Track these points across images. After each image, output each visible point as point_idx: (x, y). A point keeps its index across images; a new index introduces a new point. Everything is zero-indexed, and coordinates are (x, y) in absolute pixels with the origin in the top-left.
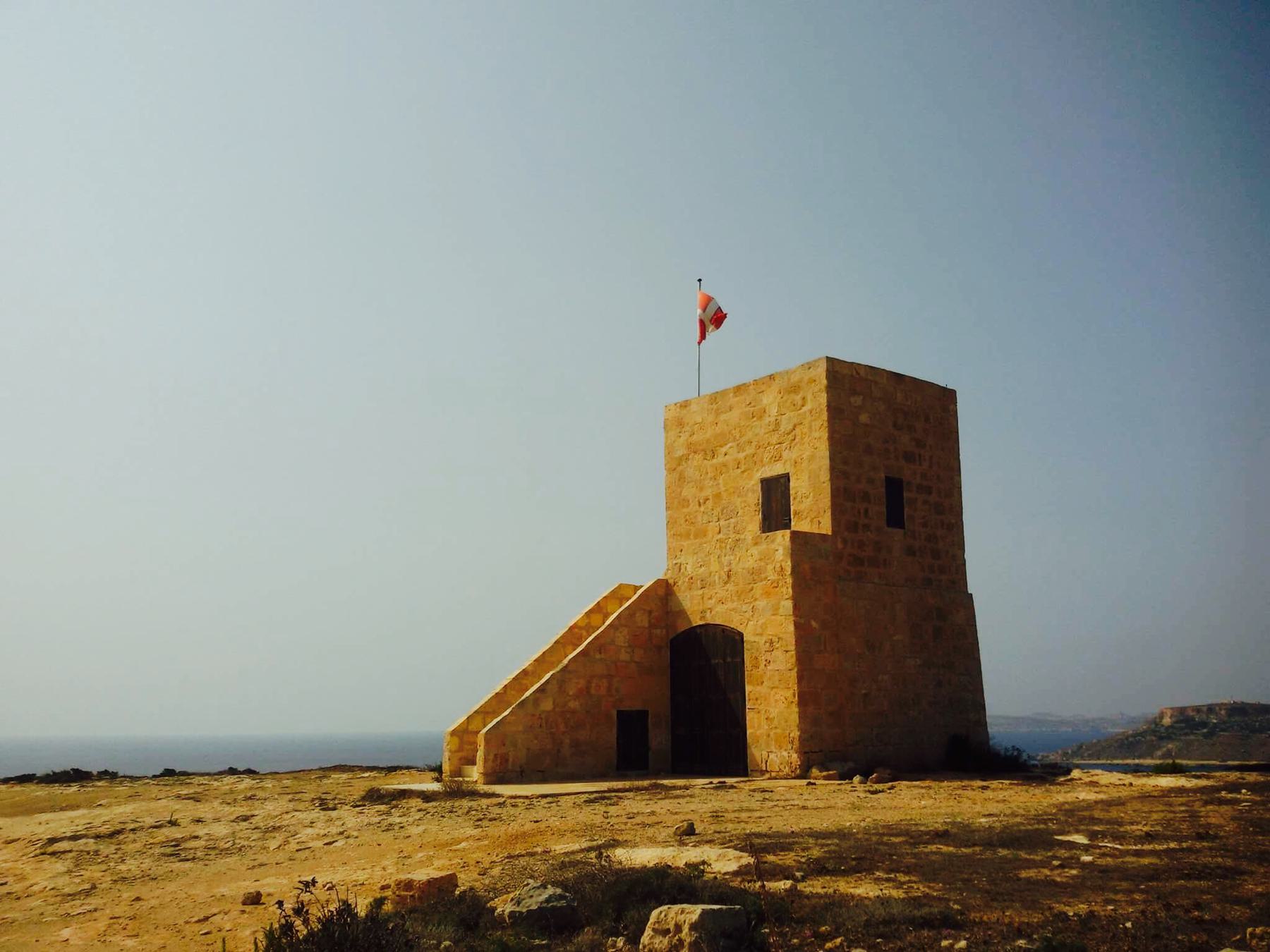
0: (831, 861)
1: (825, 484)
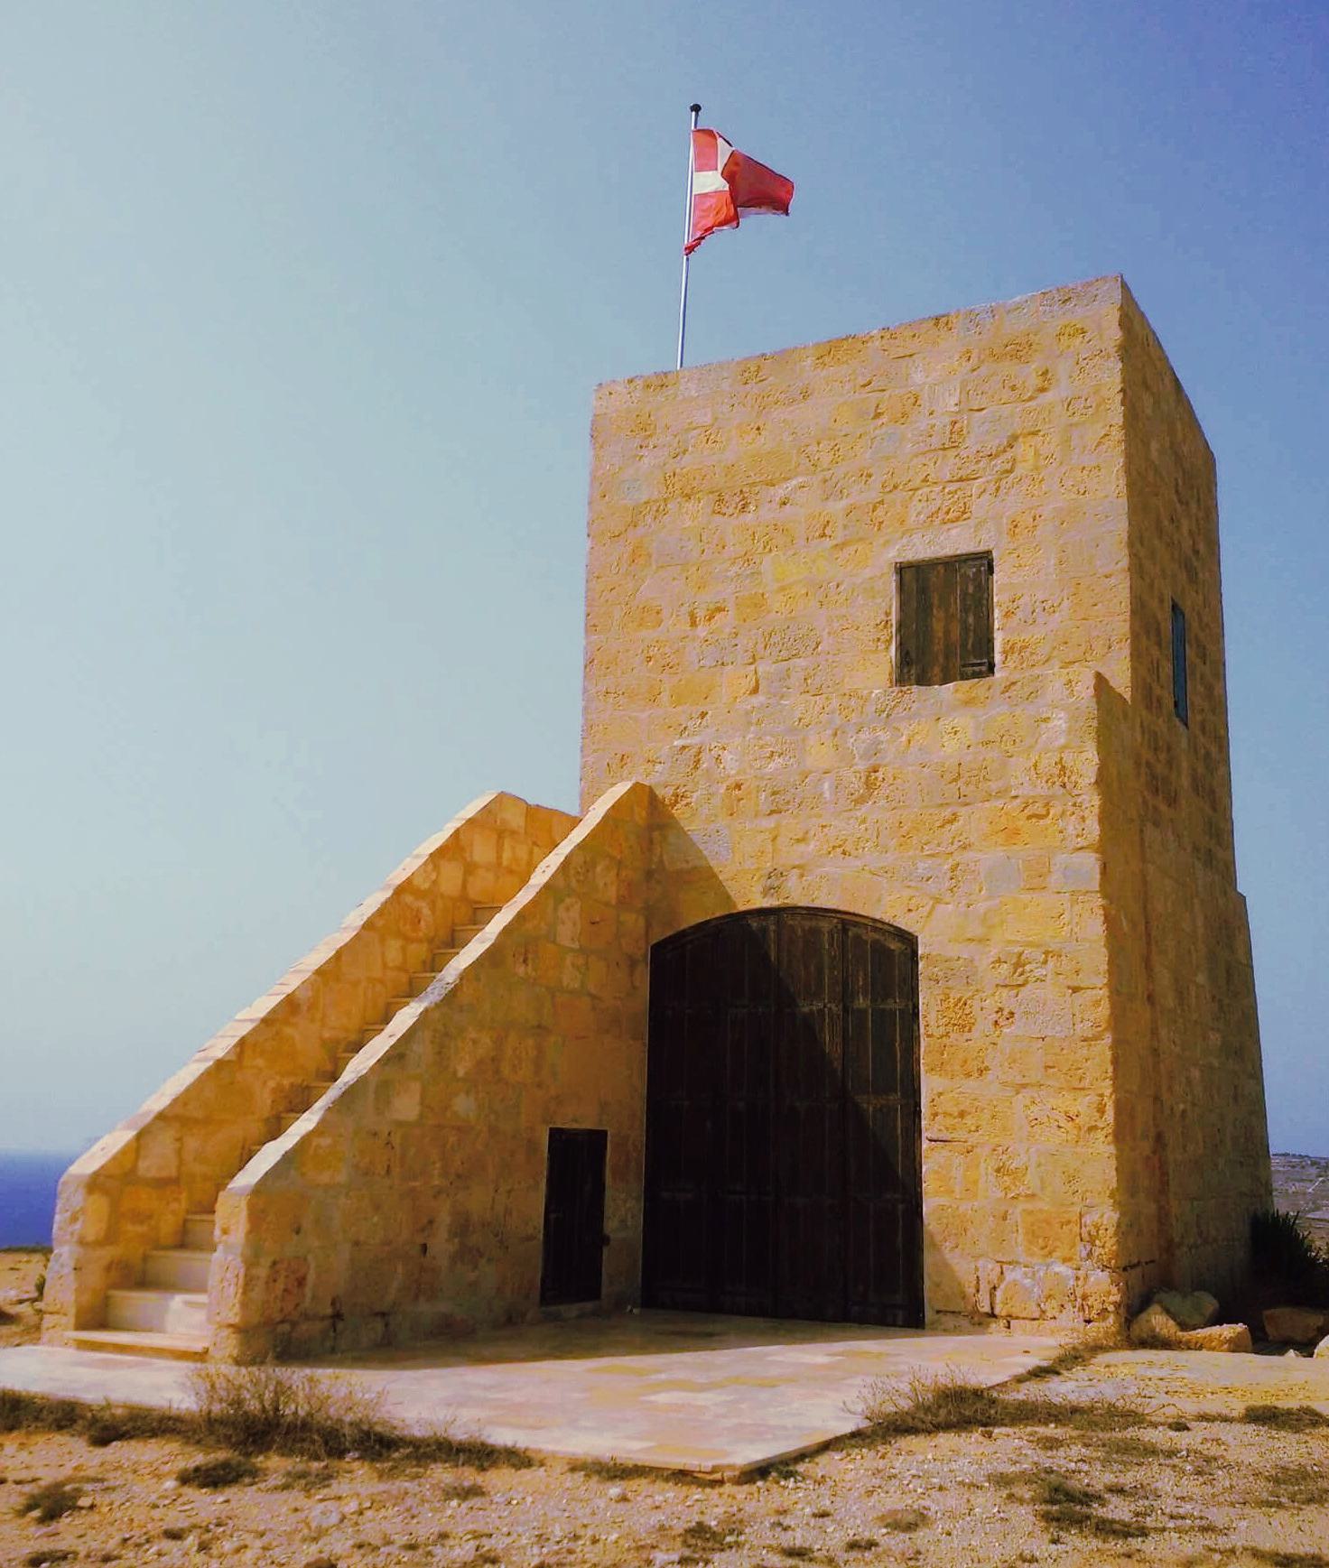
1: (1113, 581)
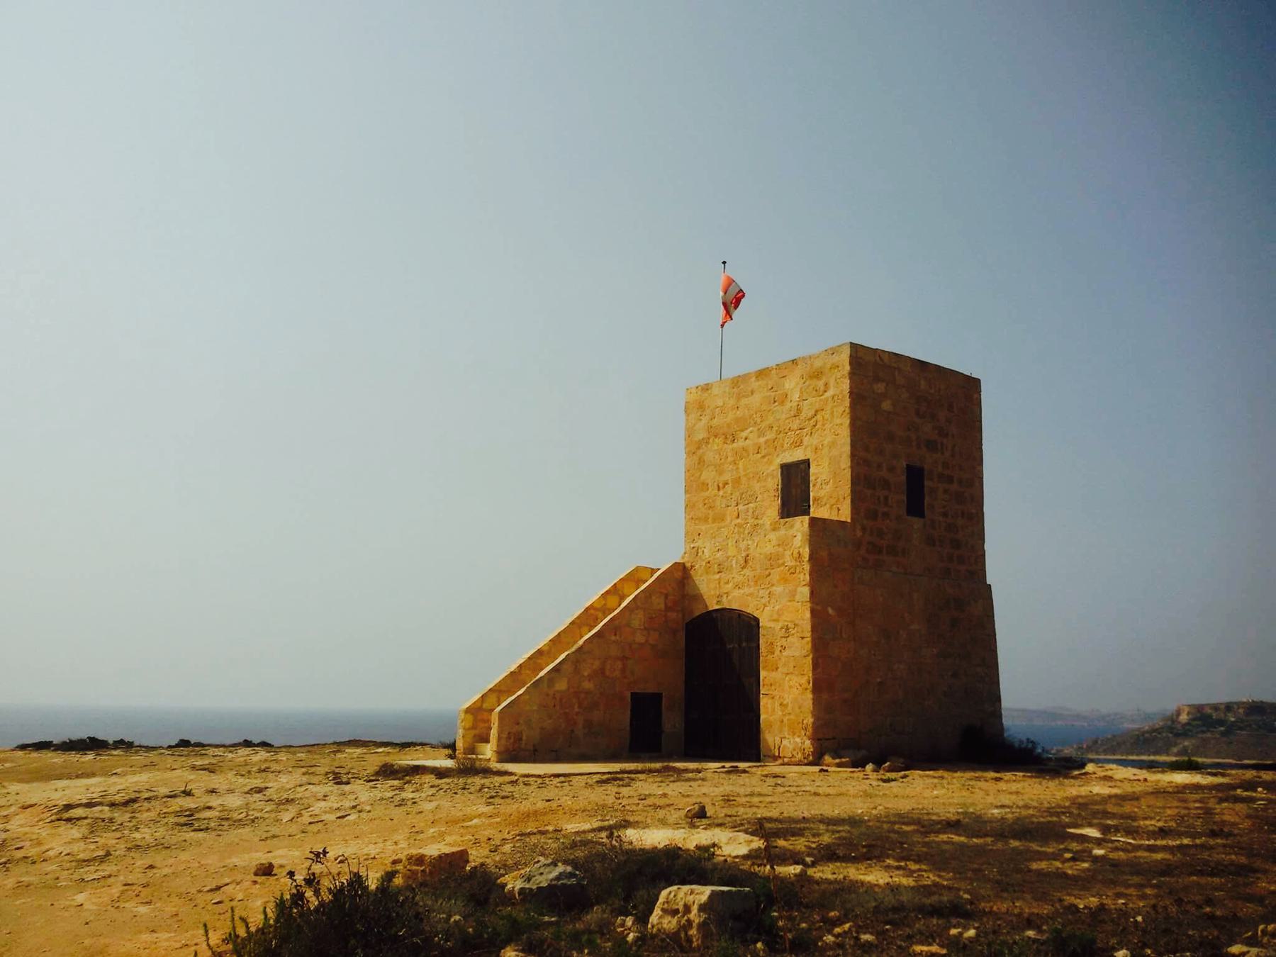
0: (841, 848)
1: (846, 471)
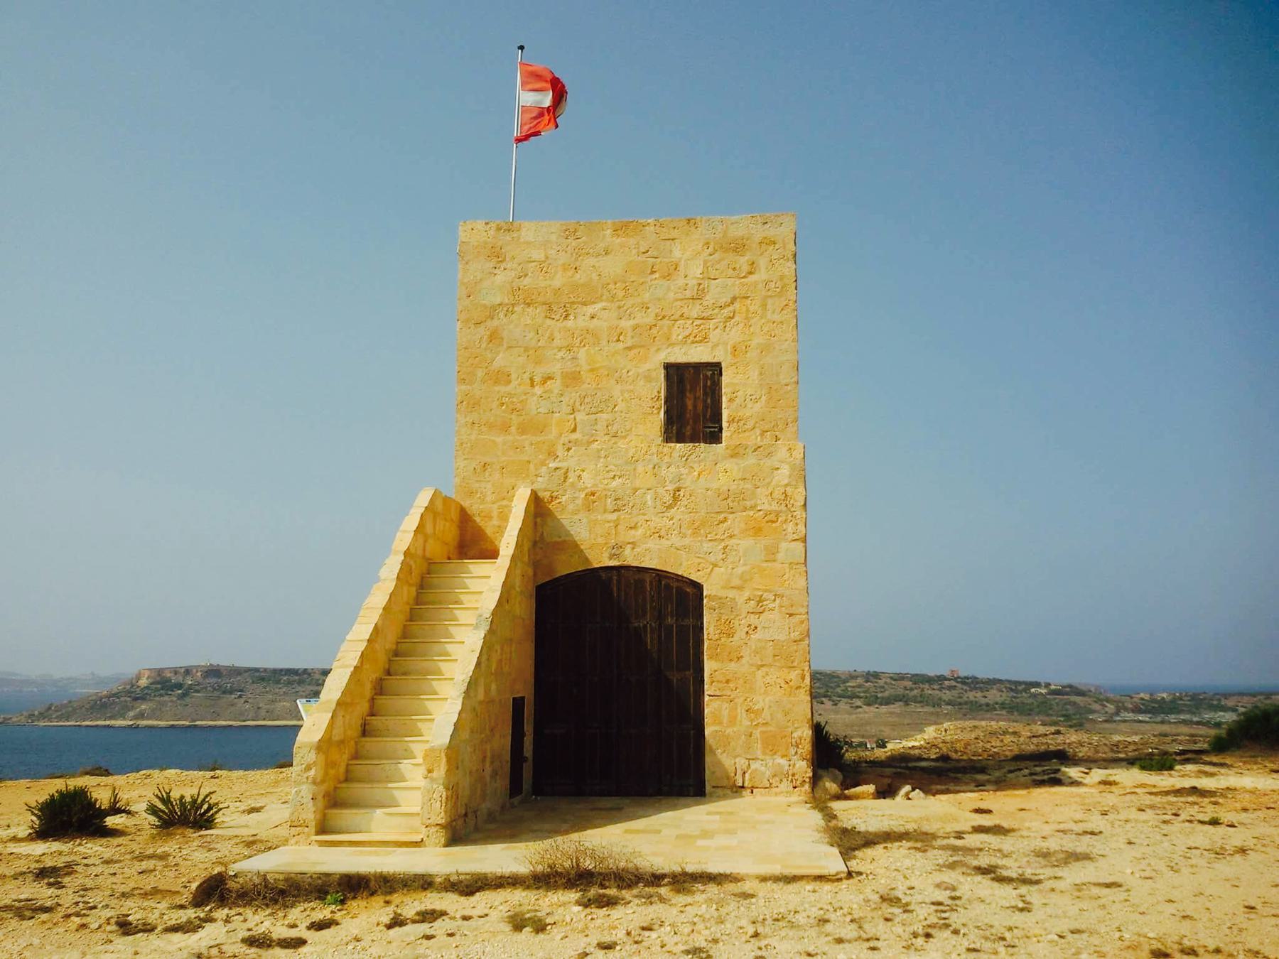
1: (789, 388)
